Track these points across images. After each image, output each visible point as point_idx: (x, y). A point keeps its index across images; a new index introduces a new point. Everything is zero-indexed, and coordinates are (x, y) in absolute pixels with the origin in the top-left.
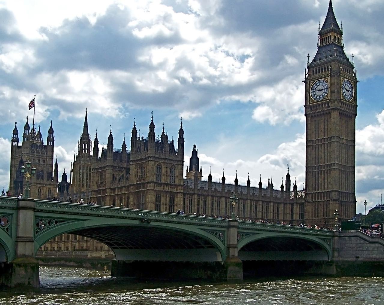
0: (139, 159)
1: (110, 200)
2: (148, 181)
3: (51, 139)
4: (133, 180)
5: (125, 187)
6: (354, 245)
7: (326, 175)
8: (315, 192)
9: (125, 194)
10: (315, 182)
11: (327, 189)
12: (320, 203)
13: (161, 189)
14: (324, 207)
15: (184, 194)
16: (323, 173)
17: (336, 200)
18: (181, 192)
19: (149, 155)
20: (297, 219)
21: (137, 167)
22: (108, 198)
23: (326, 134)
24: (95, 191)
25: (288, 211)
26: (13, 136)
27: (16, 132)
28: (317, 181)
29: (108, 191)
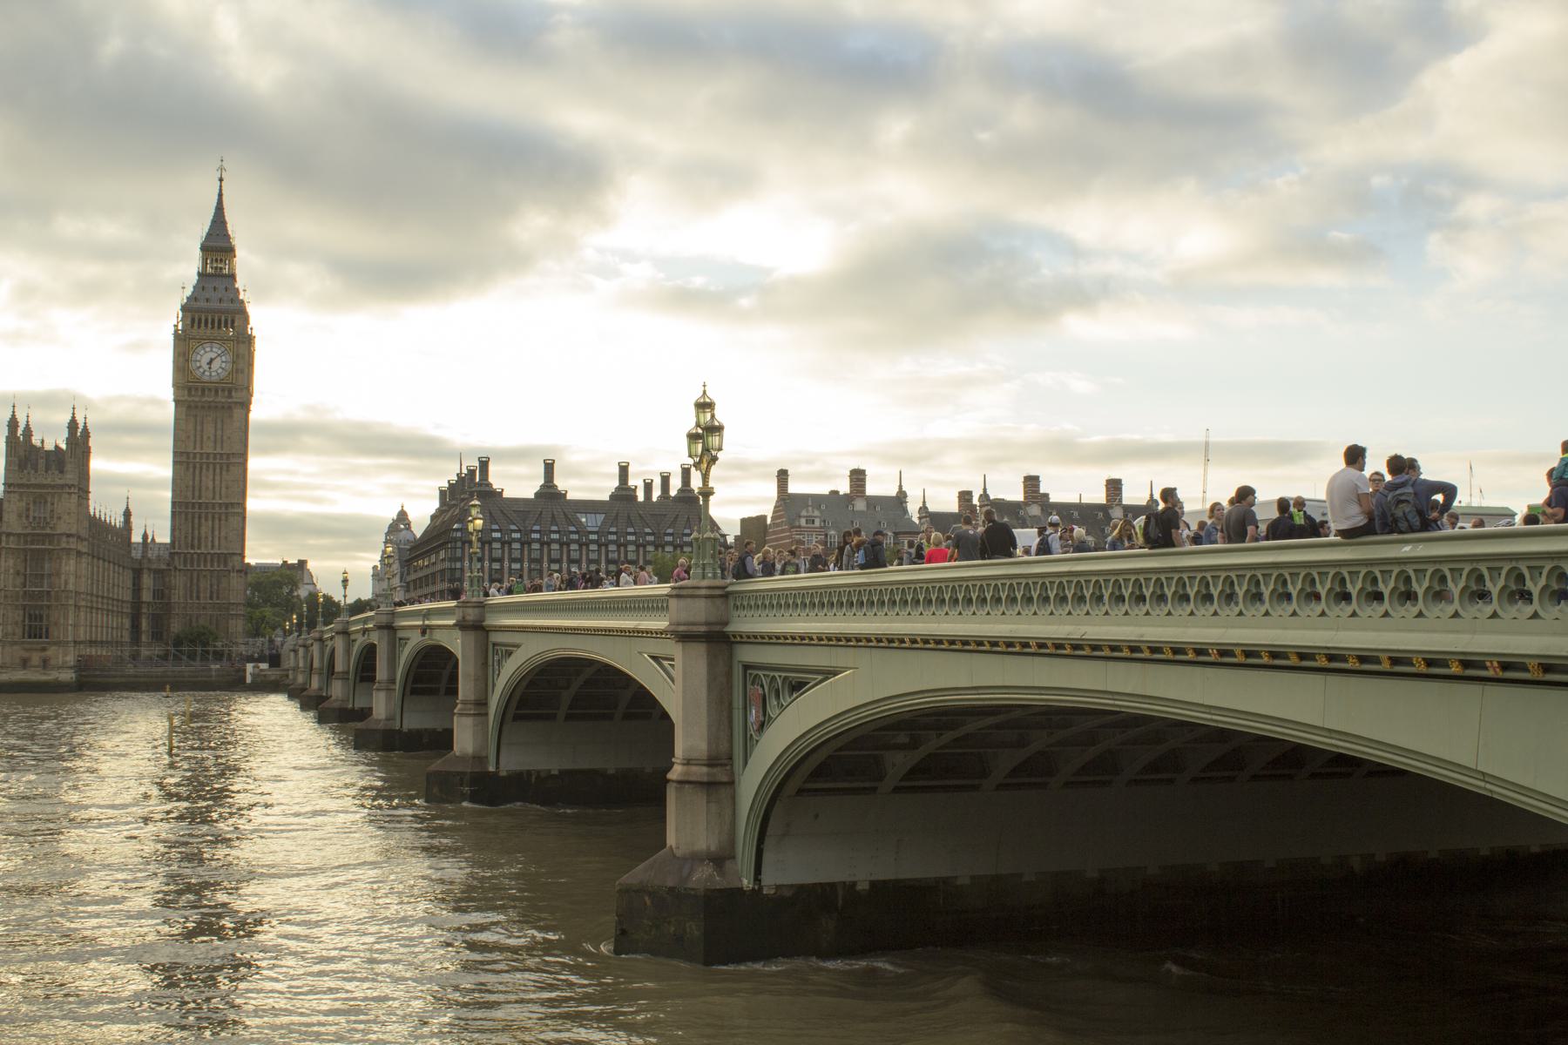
0: (32, 485)
2: (68, 532)
7: (217, 521)
8: (192, 551)
10: (193, 533)
11: (219, 549)
12: (204, 573)
14: (211, 580)
16: (210, 516)
18: (85, 553)
19: (70, 483)
20: (148, 600)
21: (25, 499)
23: (219, 445)
25: (129, 583)
28: (196, 532)
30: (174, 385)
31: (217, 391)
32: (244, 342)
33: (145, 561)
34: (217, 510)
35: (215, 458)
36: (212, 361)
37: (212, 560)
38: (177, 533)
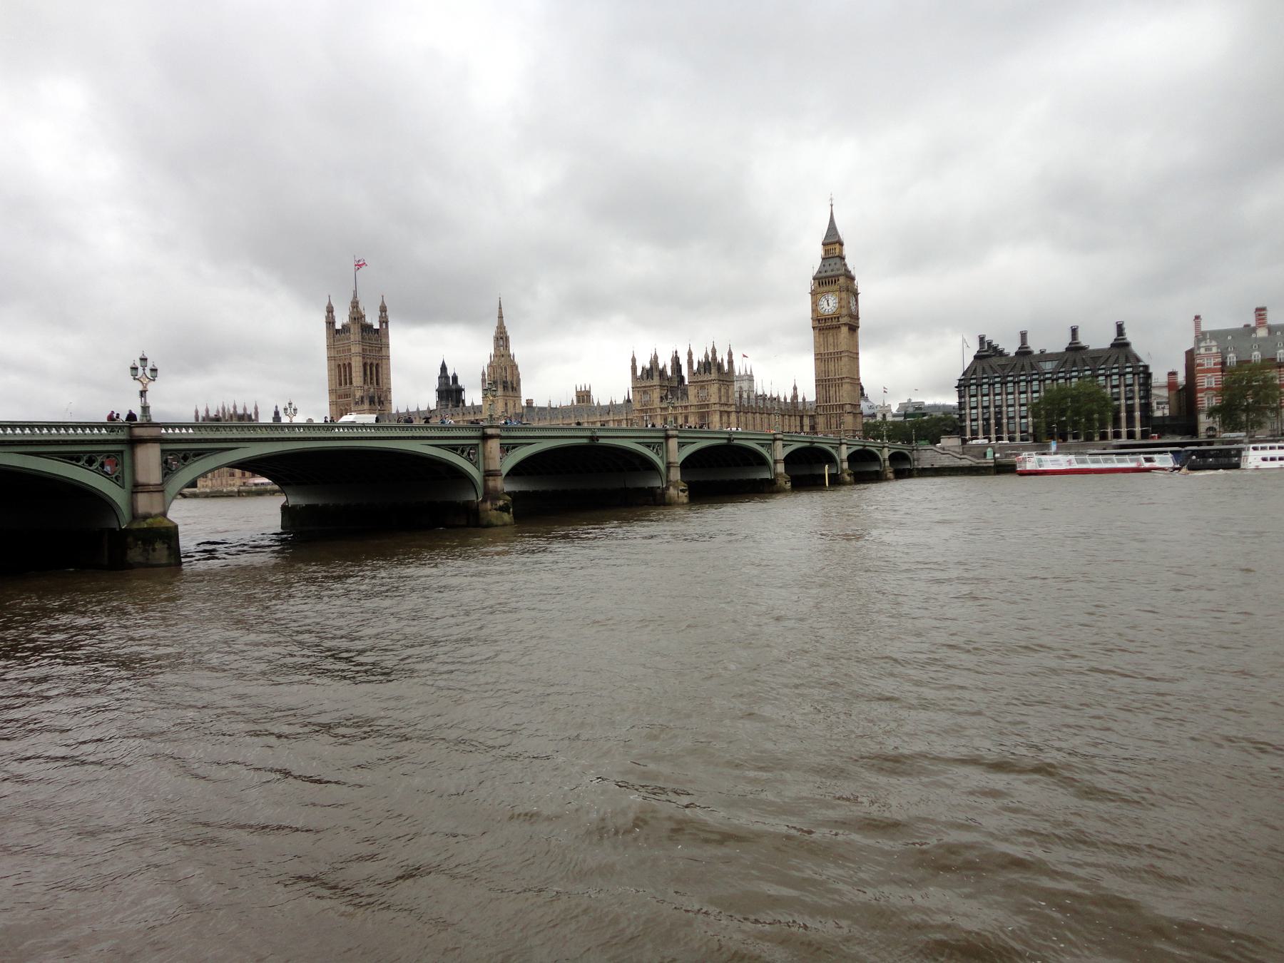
1: (661, 419)
3: (384, 321)
4: (692, 398)
5: (681, 406)
6: (929, 456)
9: (681, 413)
13: (722, 409)
15: (736, 412)
17: (850, 413)
19: (713, 378)
22: (659, 417)
24: (637, 410)
25: (798, 423)
26: (328, 315)
27: (330, 310)
29: (659, 410)
30: (812, 318)
31: (832, 319)
32: (844, 291)
33: (804, 411)
34: (837, 381)
35: (834, 355)
36: (830, 304)
37: (836, 408)
38: (818, 396)
